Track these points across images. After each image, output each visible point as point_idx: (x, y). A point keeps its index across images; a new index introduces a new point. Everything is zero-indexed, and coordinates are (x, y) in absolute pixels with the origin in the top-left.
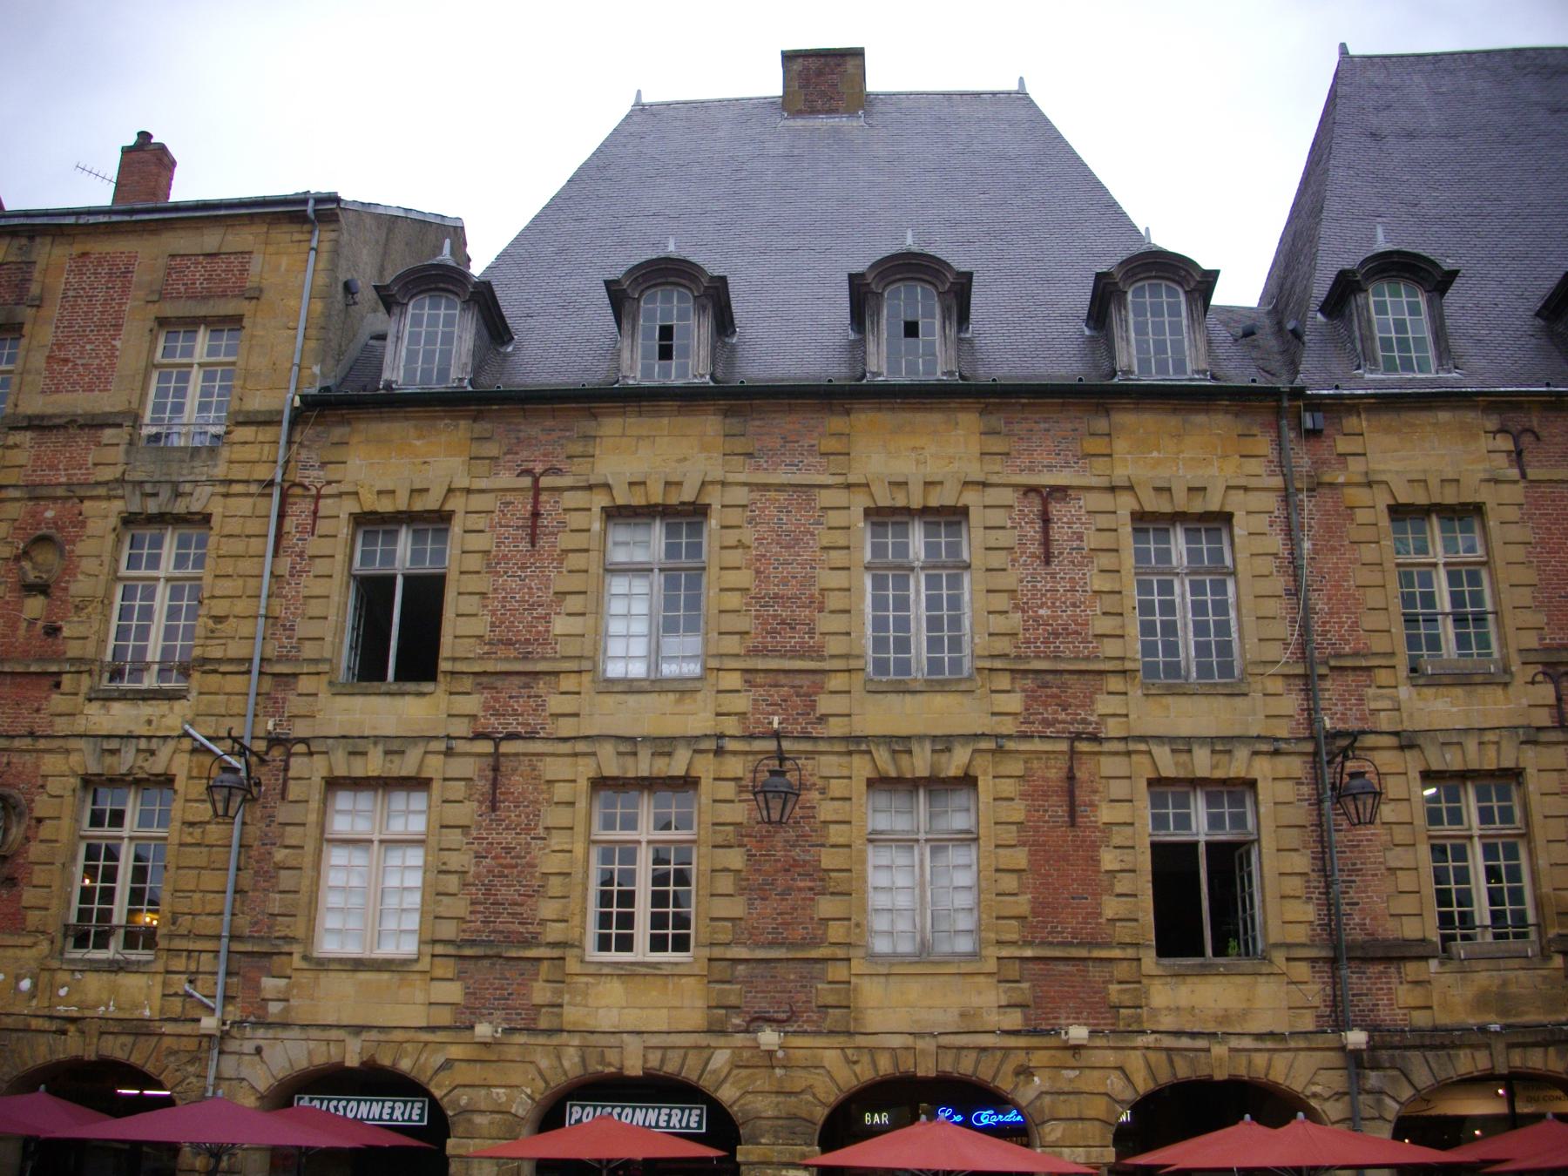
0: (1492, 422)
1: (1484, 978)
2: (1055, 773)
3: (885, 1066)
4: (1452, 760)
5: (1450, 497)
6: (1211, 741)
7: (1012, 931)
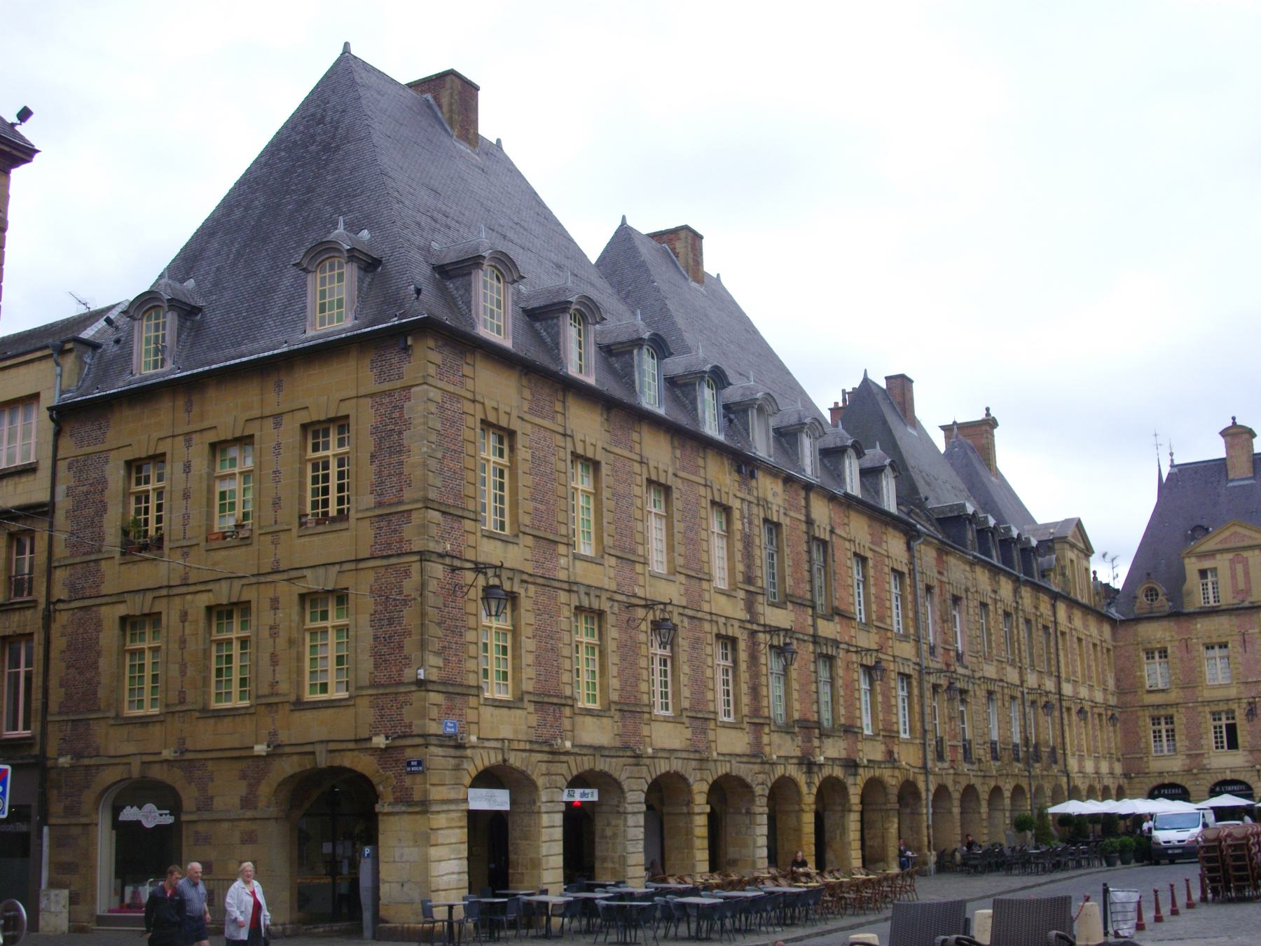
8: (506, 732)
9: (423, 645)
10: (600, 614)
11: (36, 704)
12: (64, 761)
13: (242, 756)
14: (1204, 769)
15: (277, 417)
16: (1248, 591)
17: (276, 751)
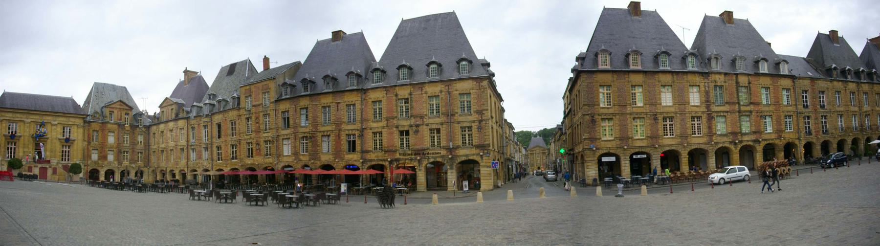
0: (384, 90)
1: (376, 154)
2: (338, 134)
3: (323, 163)
4: (375, 131)
5: (378, 100)
6: (351, 130)
7: (333, 150)
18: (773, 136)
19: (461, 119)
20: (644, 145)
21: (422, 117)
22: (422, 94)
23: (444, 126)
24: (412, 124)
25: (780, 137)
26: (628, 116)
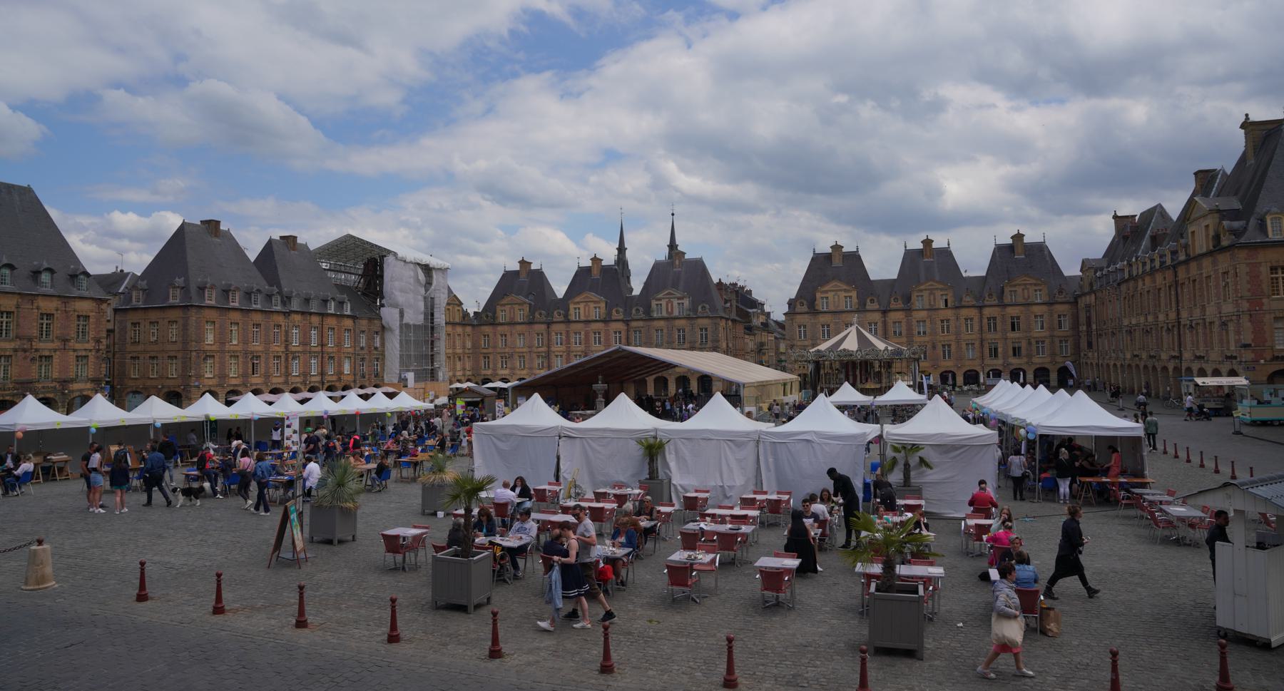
8: (211, 383)
9: (191, 369)
10: (238, 356)
11: (112, 372)
12: (119, 387)
13: (156, 387)
14: (497, 375)
15: (164, 318)
16: (513, 318)
17: (163, 387)
18: (334, 378)
19: (78, 346)
20: (237, 383)
21: (30, 340)
22: (32, 309)
23: (58, 353)
24: (17, 347)
25: (340, 379)
26: (227, 354)
